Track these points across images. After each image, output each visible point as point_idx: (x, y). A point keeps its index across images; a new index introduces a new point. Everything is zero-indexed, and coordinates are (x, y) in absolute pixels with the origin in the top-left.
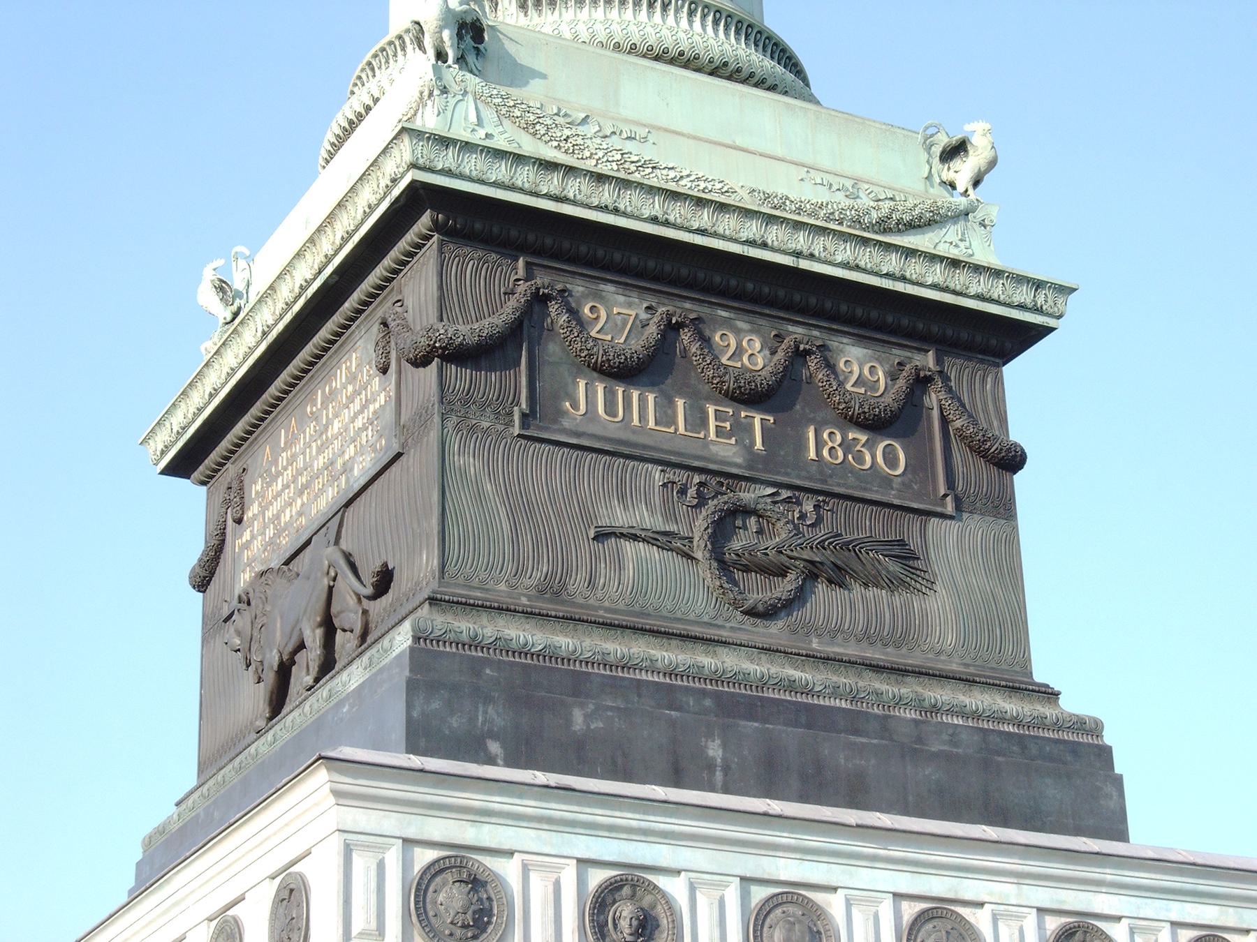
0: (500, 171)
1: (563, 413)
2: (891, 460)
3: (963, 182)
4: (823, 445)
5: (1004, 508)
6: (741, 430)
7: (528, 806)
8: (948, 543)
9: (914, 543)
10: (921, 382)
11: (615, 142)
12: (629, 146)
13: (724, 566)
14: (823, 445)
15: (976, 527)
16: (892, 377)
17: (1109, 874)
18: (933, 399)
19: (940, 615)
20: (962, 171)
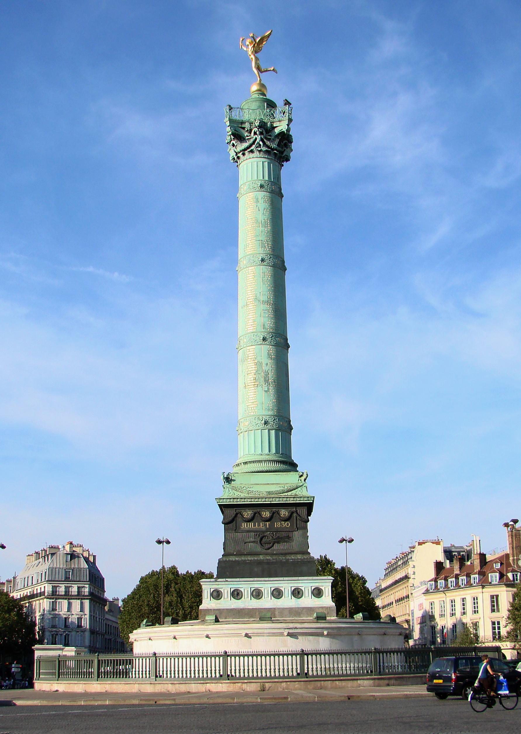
0: (229, 500)
1: (240, 528)
2: (288, 525)
3: (303, 480)
4: (277, 525)
5: (306, 528)
6: (266, 525)
7: (223, 583)
8: (297, 535)
9: (290, 535)
10: (292, 513)
11: (248, 489)
12: (250, 489)
13: (261, 544)
14: (277, 525)
15: (300, 532)
16: (288, 513)
17: (300, 581)
18: (295, 515)
19: (295, 545)
20: (303, 478)
